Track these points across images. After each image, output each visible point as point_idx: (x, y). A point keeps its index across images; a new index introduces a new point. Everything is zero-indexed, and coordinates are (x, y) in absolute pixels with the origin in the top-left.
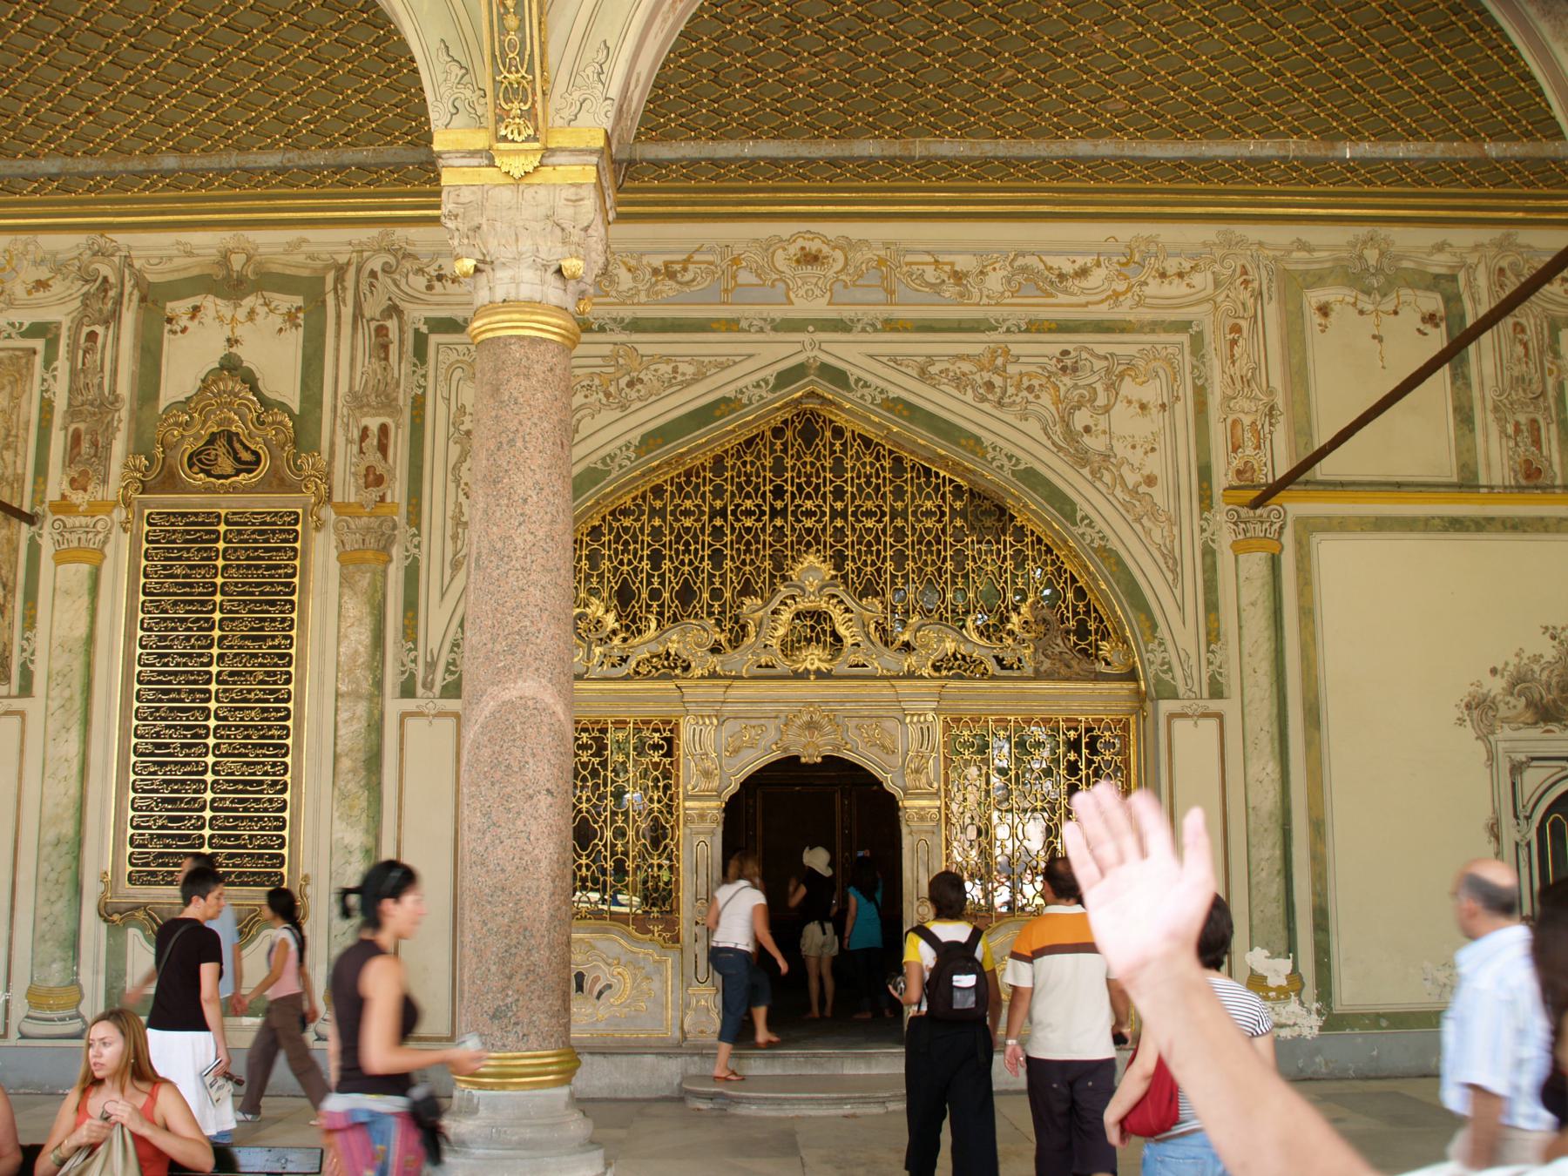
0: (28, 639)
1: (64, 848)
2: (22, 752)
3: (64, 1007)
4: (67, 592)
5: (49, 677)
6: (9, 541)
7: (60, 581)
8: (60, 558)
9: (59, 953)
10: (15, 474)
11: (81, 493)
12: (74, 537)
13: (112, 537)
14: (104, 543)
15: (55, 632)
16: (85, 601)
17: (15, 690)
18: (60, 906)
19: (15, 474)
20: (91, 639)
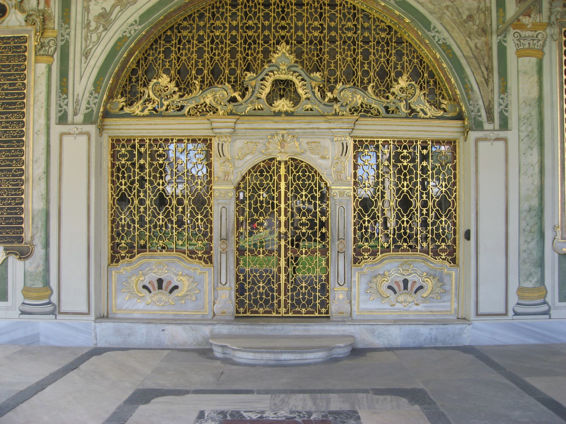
0: (503, 99)
1: (533, 213)
2: (507, 160)
3: (539, 297)
4: (525, 73)
5: (519, 120)
6: (486, 44)
7: (519, 67)
8: (520, 54)
9: (533, 270)
10: (486, 7)
11: (527, 18)
12: (526, 42)
13: (547, 43)
14: (544, 45)
15: (521, 95)
16: (535, 78)
17: (497, 126)
18: (533, 244)
19: (486, 7)
20: (540, 99)
